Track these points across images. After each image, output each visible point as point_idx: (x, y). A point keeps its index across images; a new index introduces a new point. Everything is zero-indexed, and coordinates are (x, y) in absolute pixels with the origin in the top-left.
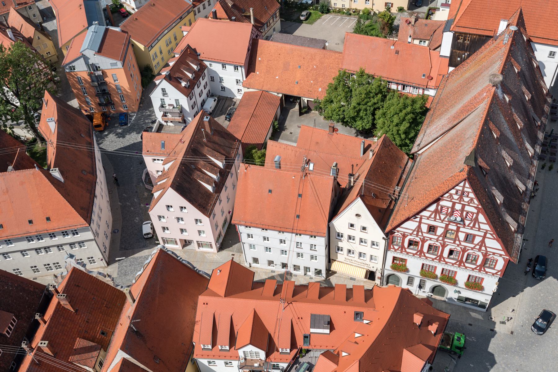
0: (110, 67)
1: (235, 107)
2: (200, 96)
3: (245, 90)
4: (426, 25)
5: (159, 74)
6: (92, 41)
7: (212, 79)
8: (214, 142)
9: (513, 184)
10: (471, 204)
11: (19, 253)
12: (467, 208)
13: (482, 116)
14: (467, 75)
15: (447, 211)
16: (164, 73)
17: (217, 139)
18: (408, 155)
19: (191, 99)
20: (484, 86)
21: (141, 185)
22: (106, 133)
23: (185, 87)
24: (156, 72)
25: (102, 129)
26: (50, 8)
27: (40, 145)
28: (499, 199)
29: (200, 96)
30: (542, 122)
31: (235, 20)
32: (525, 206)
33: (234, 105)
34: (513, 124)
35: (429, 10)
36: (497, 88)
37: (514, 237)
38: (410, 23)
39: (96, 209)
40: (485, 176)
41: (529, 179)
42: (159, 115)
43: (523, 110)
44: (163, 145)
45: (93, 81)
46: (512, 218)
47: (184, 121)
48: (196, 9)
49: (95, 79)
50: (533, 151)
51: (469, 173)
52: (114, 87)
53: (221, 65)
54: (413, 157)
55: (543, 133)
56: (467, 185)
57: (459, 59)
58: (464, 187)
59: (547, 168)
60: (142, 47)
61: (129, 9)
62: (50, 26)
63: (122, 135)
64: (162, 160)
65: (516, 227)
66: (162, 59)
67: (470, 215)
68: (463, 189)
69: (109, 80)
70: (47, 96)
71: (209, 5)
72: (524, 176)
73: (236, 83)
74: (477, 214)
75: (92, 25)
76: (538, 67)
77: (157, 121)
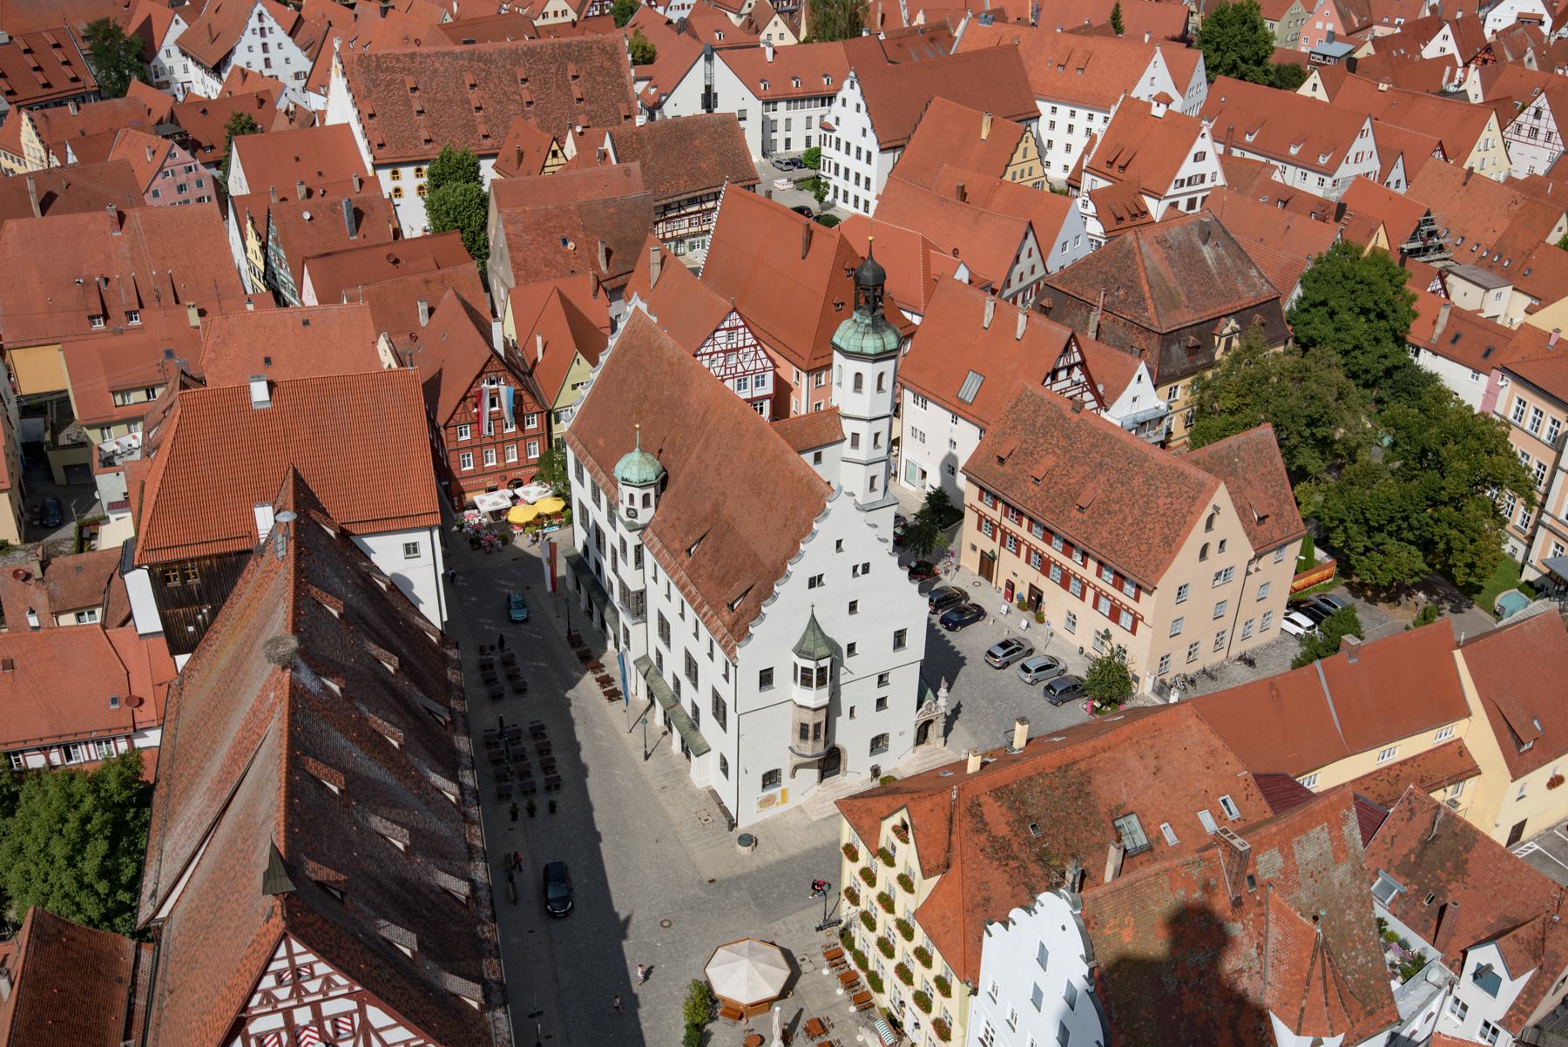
4: (79, 569)
9: (431, 889)
10: (331, 994)
12: (328, 1009)
13: (279, 751)
14: (223, 661)
15: (280, 1041)
18: (133, 936)
20: (265, 677)
28: (406, 944)
30: (452, 711)
32: (486, 931)
34: (376, 743)
35: (81, 528)
36: (295, 669)
37: (487, 1024)
38: (28, 576)
40: (342, 901)
41: (471, 859)
43: (390, 699)
46: (462, 976)
50: (454, 788)
51: (290, 917)
54: (147, 935)
55: (468, 734)
56: (297, 947)
57: (191, 629)
58: (290, 955)
59: (522, 813)
65: (479, 995)
67: (344, 1024)
68: (292, 963)
72: (454, 857)
74: (362, 1010)
76: (393, 587)
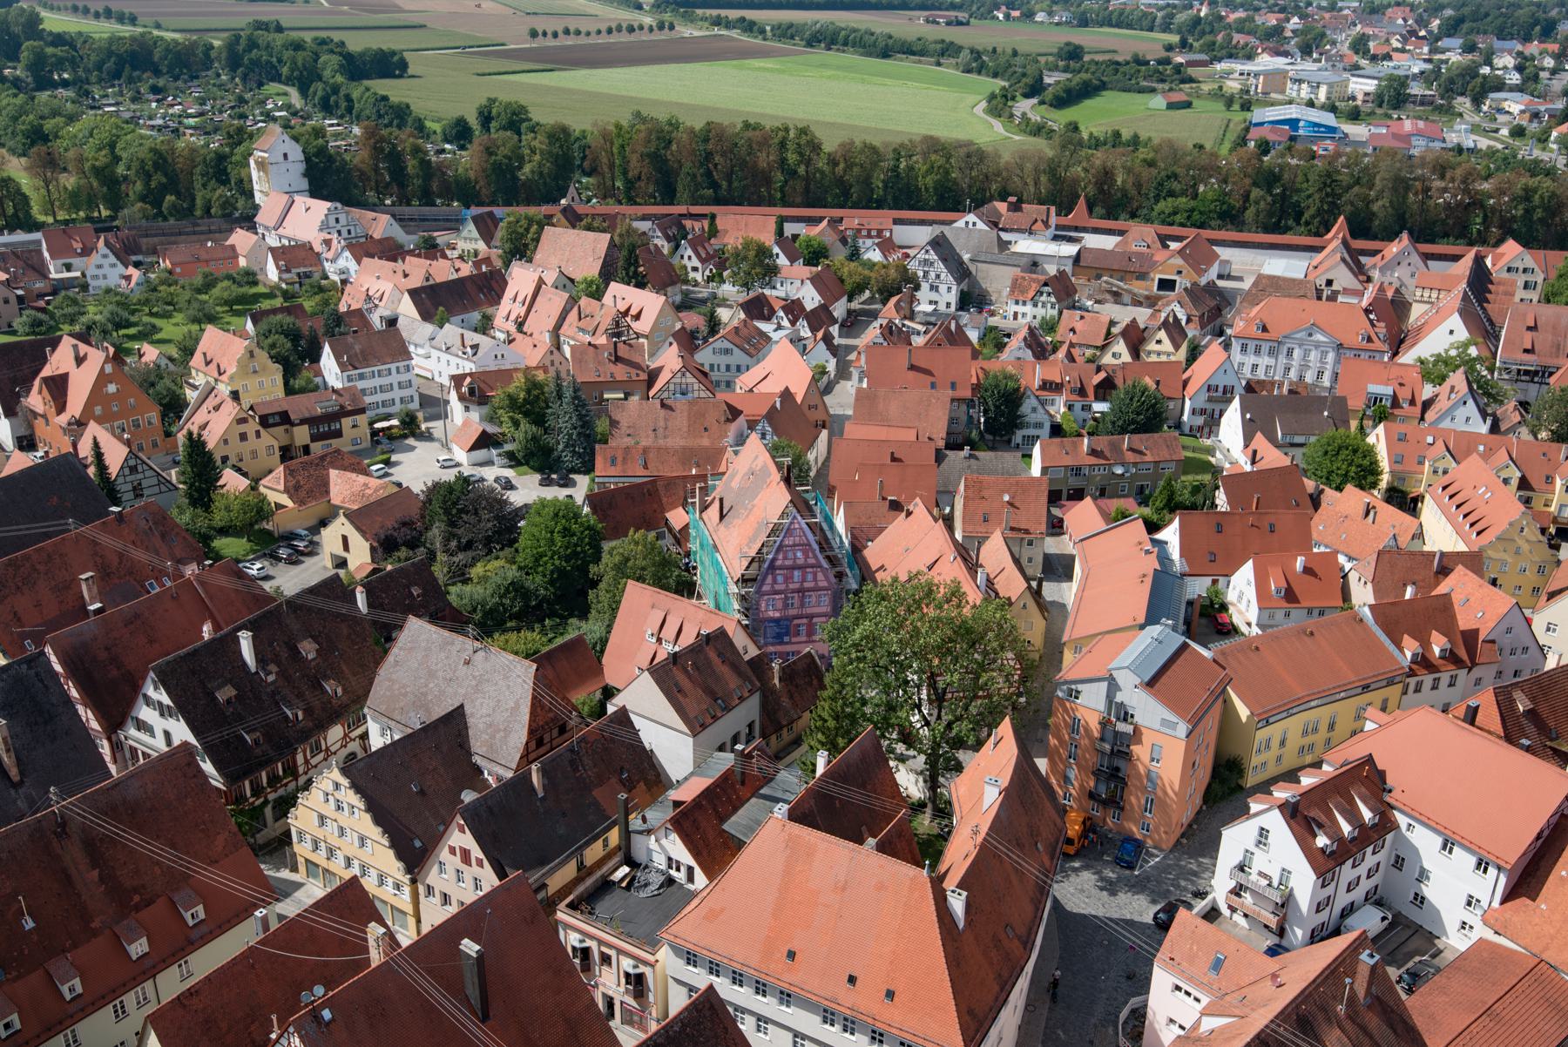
0: (1157, 726)
1: (1436, 961)
2: (1349, 890)
3: (1481, 932)
5: (1265, 788)
6: (1144, 657)
7: (1399, 863)
8: (1363, 1029)
11: (790, 1035)
16: (1282, 793)
17: (1374, 1022)
19: (1323, 886)
21: (1111, 1030)
22: (1077, 865)
23: (1323, 850)
24: (1251, 780)
25: (1071, 850)
26: (1072, 558)
27: (926, 822)
29: (1349, 890)
31: (1528, 749)
33: (1434, 956)
39: (993, 1032)
42: (1220, 885)
44: (1217, 965)
45: (1102, 739)
47: (1281, 932)
48: (1412, 681)
49: (1109, 736)
52: (1142, 770)
53: (1439, 841)
60: (1243, 712)
61: (1237, 620)
62: (1050, 591)
63: (1111, 888)
64: (1197, 1000)
66: (1279, 759)
69: (1140, 751)
70: (1005, 728)
71: (1450, 685)
73: (1464, 901)
75: (1157, 622)
77: (1210, 897)
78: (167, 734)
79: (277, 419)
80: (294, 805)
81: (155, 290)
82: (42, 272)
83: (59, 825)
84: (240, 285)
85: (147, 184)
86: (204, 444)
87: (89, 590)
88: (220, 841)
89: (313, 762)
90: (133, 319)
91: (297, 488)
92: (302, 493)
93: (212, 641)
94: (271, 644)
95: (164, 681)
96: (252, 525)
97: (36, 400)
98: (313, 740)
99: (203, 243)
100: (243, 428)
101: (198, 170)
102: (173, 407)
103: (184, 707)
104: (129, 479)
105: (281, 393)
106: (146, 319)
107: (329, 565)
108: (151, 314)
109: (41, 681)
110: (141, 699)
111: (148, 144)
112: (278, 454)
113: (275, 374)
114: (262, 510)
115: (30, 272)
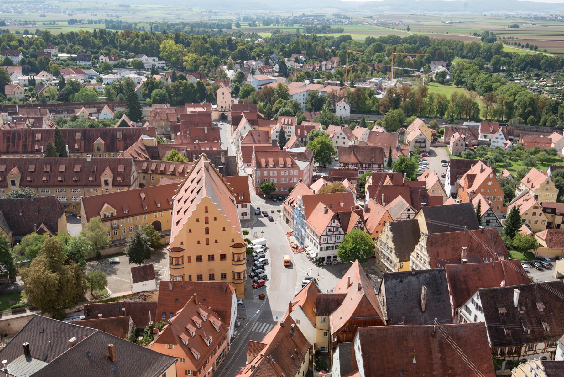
78: (476, 317)
79: (550, 211)
80: (516, 366)
81: (515, 150)
82: (476, 138)
83: (434, 332)
84: (549, 154)
85: (524, 110)
86: (519, 212)
87: (464, 253)
88: (485, 366)
89: (528, 353)
90: (503, 160)
91: (551, 240)
92: (552, 243)
93: (503, 289)
94: (526, 299)
95: (482, 296)
96: (527, 249)
97: (462, 181)
98: (531, 344)
99: (539, 136)
100: (535, 210)
101: (546, 107)
102: (509, 196)
103: (487, 309)
104: (486, 218)
105: (554, 200)
106: (508, 161)
107: (555, 276)
108: (510, 159)
109: (441, 279)
110: (470, 300)
111: (529, 95)
112: (546, 224)
113: (556, 192)
114: (533, 245)
115: (472, 137)
